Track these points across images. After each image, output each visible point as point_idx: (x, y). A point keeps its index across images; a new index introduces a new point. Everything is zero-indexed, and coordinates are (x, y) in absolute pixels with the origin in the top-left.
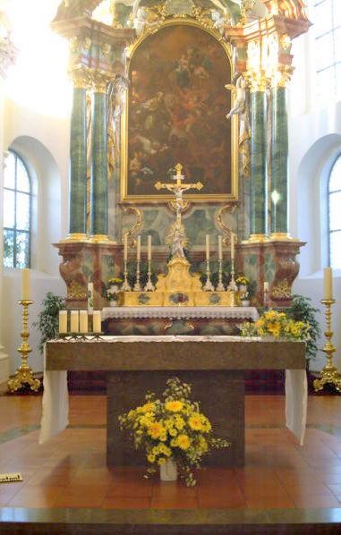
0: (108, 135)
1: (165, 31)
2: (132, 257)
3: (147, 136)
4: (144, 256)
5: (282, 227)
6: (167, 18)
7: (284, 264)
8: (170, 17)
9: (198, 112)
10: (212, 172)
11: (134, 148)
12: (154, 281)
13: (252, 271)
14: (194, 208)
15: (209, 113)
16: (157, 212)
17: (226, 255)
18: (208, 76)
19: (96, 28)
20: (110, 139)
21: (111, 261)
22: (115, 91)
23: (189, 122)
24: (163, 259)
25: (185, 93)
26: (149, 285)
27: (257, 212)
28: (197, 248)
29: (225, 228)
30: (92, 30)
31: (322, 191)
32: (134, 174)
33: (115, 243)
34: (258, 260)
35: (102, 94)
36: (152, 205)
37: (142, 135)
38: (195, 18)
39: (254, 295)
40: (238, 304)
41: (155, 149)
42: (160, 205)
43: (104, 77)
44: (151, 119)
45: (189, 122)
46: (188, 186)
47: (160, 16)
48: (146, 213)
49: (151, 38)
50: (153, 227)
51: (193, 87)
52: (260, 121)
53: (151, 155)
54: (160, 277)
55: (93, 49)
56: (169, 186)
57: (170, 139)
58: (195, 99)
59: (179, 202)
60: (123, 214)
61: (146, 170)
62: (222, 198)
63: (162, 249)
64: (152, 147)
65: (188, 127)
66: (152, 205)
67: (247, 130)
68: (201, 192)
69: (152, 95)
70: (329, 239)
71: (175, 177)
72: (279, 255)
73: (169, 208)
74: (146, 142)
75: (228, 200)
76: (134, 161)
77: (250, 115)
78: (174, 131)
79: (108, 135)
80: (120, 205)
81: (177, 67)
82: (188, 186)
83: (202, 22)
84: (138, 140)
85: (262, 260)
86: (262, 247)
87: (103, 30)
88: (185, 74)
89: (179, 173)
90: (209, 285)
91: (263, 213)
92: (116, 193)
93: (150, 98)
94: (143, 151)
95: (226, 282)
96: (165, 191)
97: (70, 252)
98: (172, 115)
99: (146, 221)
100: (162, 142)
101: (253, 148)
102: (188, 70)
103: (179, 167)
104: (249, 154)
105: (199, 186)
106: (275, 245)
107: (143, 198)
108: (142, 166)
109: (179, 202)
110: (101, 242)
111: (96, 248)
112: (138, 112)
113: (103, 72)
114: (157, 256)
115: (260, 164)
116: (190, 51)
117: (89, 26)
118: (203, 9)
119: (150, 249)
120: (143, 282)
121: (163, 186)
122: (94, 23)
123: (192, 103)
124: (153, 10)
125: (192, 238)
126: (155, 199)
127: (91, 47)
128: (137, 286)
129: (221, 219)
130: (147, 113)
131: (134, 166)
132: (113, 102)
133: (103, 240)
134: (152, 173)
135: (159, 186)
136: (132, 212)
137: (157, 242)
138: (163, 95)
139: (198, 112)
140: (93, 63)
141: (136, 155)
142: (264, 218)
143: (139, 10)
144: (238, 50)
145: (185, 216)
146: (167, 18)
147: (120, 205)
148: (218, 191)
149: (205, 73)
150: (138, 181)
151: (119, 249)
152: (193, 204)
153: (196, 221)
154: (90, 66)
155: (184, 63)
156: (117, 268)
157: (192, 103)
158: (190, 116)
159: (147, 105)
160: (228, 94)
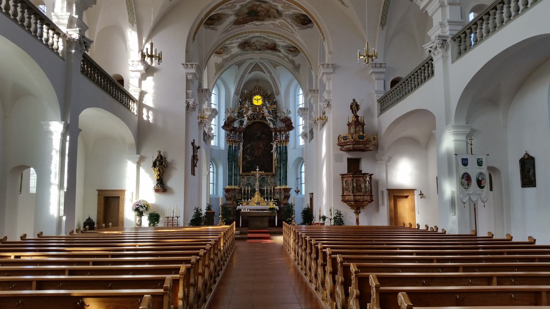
1: (253, 123)
2: (245, 191)
4: (248, 191)
5: (286, 184)
7: (286, 194)
11: (244, 158)
12: (251, 199)
17: (271, 190)
23: (261, 150)
24: (254, 191)
26: (249, 200)
31: (299, 172)
39: (278, 203)
43: (237, 142)
45: (261, 150)
54: (253, 198)
59: (258, 176)
72: (284, 192)
74: (248, 157)
86: (280, 189)
90: (266, 200)
95: (271, 200)
97: (227, 191)
103: (258, 167)
104: (277, 163)
107: (247, 173)
109: (258, 176)
111: (235, 189)
115: (279, 166)
120: (248, 200)
123: (261, 145)
128: (246, 200)
129: (269, 180)
130: (248, 148)
132: (239, 148)
133: (237, 187)
137: (251, 187)
147: (240, 175)
153: (262, 180)
156: (240, 195)
159: (248, 146)
160: (272, 146)
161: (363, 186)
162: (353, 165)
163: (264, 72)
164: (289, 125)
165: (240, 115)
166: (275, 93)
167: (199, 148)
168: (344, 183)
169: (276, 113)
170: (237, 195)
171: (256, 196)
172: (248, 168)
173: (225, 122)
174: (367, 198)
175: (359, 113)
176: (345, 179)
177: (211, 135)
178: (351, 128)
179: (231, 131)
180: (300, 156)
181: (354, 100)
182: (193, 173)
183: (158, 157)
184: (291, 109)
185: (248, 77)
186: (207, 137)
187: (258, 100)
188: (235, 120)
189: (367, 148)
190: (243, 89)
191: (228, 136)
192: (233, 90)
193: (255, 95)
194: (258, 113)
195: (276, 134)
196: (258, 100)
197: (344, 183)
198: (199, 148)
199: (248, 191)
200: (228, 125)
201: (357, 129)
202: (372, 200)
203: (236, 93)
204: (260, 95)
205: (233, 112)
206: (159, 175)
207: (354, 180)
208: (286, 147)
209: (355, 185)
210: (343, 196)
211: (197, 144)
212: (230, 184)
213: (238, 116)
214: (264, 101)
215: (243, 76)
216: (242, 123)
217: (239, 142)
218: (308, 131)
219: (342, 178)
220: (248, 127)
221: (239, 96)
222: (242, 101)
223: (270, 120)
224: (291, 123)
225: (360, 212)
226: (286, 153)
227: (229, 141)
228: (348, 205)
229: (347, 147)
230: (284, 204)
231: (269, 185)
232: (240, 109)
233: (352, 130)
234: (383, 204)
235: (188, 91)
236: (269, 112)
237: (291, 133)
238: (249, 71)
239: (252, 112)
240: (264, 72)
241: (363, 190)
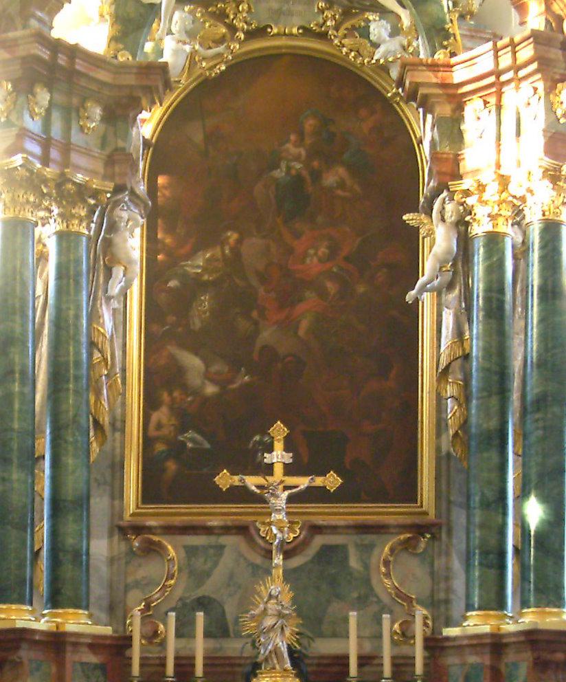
0: (92, 345)
1: (244, 71)
6: (251, 35)
8: (261, 32)
9: (331, 287)
11: (160, 379)
14: (319, 541)
15: (361, 289)
16: (221, 548)
18: (357, 188)
19: (62, 60)
20: (97, 355)
22: (113, 227)
23: (306, 312)
25: (297, 235)
27: (485, 553)
30: (52, 67)
32: (160, 447)
35: (79, 234)
36: (208, 530)
37: (183, 346)
38: (323, 36)
41: (214, 381)
42: (226, 530)
43: (83, 191)
44: (205, 302)
45: (306, 312)
46: (303, 482)
47: (233, 29)
48: (191, 551)
49: (206, 95)
50: (206, 590)
51: (320, 219)
52: (496, 311)
53: (206, 400)
56: (252, 482)
57: (255, 355)
58: (323, 250)
59: (279, 524)
60: (131, 553)
61: (191, 438)
63: (233, 647)
64: (208, 376)
65: (304, 325)
66: (208, 530)
67: (459, 333)
68: (340, 496)
71: (268, 458)
73: (251, 541)
74: (193, 362)
75: (408, 520)
76: (161, 415)
77: (467, 296)
78: (267, 335)
79: (92, 345)
81: (277, 166)
82: (303, 482)
84: (172, 357)
87: (80, 66)
88: (297, 182)
89: (279, 446)
92: (113, 498)
94: (185, 388)
96: (240, 495)
98: (261, 291)
99: (191, 573)
100: (236, 364)
102: (305, 173)
103: (279, 431)
105: (332, 481)
108: (183, 429)
109: (279, 524)
112: (173, 284)
113: (80, 177)
115: (493, 423)
116: (310, 124)
117: (45, 54)
118: (347, 14)
119: (199, 647)
121: (236, 480)
122: (57, 46)
123: (313, 258)
124: (213, 15)
126: (215, 515)
127: (48, 111)
130: (194, 286)
131: (159, 426)
132: (106, 256)
134: (207, 445)
135: (225, 480)
136: (152, 550)
138: (239, 242)
139: (331, 287)
140: (54, 154)
141: (165, 397)
142: (502, 567)
143: (177, 15)
146: (251, 35)
148: (381, 496)
149: (349, 182)
150: (171, 466)
152: (315, 529)
154: (45, 161)
155: (294, 155)
157: (313, 258)
159: (197, 265)
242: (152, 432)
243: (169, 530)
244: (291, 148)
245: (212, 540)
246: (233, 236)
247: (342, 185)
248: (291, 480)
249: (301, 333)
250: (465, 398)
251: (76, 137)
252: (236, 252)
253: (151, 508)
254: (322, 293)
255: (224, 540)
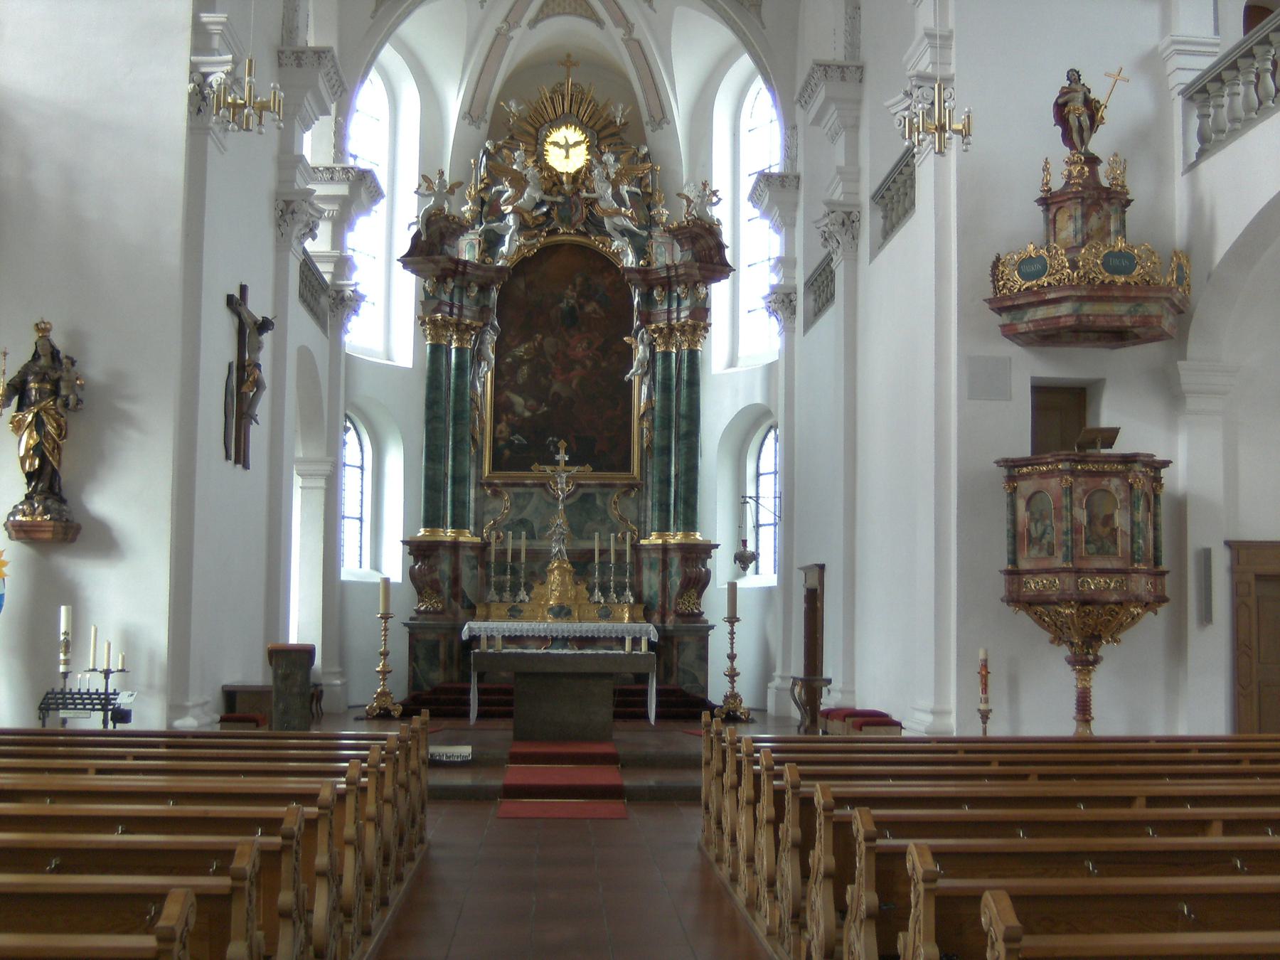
0: (472, 400)
1: (546, 251)
3: (520, 394)
4: (516, 554)
5: (690, 523)
9: (589, 363)
10: (602, 442)
11: (501, 408)
12: (529, 589)
13: (651, 581)
14: (581, 491)
15: (604, 364)
16: (531, 494)
17: (620, 555)
21: (474, 562)
22: (482, 343)
26: (522, 595)
28: (584, 545)
29: (621, 518)
33: (478, 540)
34: (659, 567)
37: (513, 391)
40: (633, 619)
46: (574, 469)
48: (517, 495)
50: (526, 514)
54: (537, 589)
55: (456, 291)
56: (548, 469)
58: (584, 345)
59: (562, 487)
61: (517, 439)
62: (618, 478)
63: (538, 545)
64: (525, 407)
65: (575, 383)
66: (525, 485)
67: (649, 397)
69: (527, 338)
70: (757, 534)
71: (558, 457)
74: (518, 400)
77: (653, 379)
78: (556, 387)
79: (472, 400)
80: (482, 485)
81: (561, 301)
83: (595, 241)
85: (665, 565)
86: (665, 549)
88: (573, 308)
89: (562, 452)
90: (598, 595)
91: (668, 506)
93: (523, 341)
94: (514, 413)
95: (620, 591)
97: (418, 550)
101: (657, 423)
103: (562, 444)
104: (651, 429)
106: (681, 547)
108: (513, 434)
109: (562, 487)
110: (461, 539)
111: (455, 546)
114: (533, 555)
116: (579, 280)
119: (523, 544)
120: (515, 590)
123: (579, 349)
125: (577, 531)
128: (507, 596)
130: (519, 362)
131: (501, 432)
132: (478, 356)
133: (467, 537)
137: (531, 536)
138: (543, 339)
139: (589, 363)
140: (455, 311)
144: (641, 295)
145: (570, 501)
147: (480, 485)
148: (612, 468)
150: (507, 453)
151: (483, 548)
152: (579, 486)
153: (583, 507)
155: (570, 297)
157: (579, 349)
158: (578, 367)
159: (520, 351)
161: (1121, 520)
162: (1063, 414)
163: (600, 23)
164: (708, 255)
165: (489, 208)
166: (645, 118)
167: (264, 326)
168: (1021, 504)
169: (650, 209)
170: (466, 571)
171: (555, 577)
172: (520, 451)
173: (416, 238)
174: (1141, 585)
175: (1098, 144)
176: (1026, 487)
177: (348, 292)
178: (1062, 218)
179: (441, 279)
180: (758, 399)
181: (1074, 76)
182: (239, 452)
183: (36, 356)
184: (720, 180)
185: (526, 42)
186: (329, 300)
187: (567, 147)
188: (461, 228)
189: (1146, 321)
190: (503, 96)
191: (429, 306)
192: (454, 101)
193: (557, 123)
194: (568, 199)
195: (647, 298)
196: (567, 147)
197: (1021, 504)
198: (264, 326)
199: (516, 554)
200: (430, 250)
201: (1094, 221)
202: (1162, 600)
203: (470, 114)
204: (583, 126)
205: (452, 191)
206: (37, 450)
207: (1079, 491)
208: (693, 355)
209: (1082, 516)
210: (1014, 573)
211: (258, 307)
212: (432, 519)
213: (478, 218)
214: (595, 149)
215: (501, 39)
216: (491, 242)
217: (481, 333)
218: (800, 281)
219: (1011, 479)
220: (523, 265)
221: (485, 127)
222: (498, 149)
223: (624, 232)
224: (721, 247)
225: (1097, 661)
226: (693, 383)
227: (434, 322)
228: (1040, 620)
229: (1041, 313)
230: (680, 615)
231: (614, 529)
232: (487, 188)
233: (1068, 229)
234: (1206, 617)
235: (206, 17)
236: (617, 196)
237: (719, 292)
238: (531, 13)
239: (538, 196)
240: (600, 23)
241: (1123, 543)
242: (497, 435)
243: (506, 485)
244: (569, 292)
245: (528, 490)
246: (539, 336)
247: (595, 311)
248: (570, 468)
249: (574, 385)
250: (651, 428)
251: (465, 302)
252: (541, 345)
253: (498, 473)
254: (584, 367)
255: (533, 490)
